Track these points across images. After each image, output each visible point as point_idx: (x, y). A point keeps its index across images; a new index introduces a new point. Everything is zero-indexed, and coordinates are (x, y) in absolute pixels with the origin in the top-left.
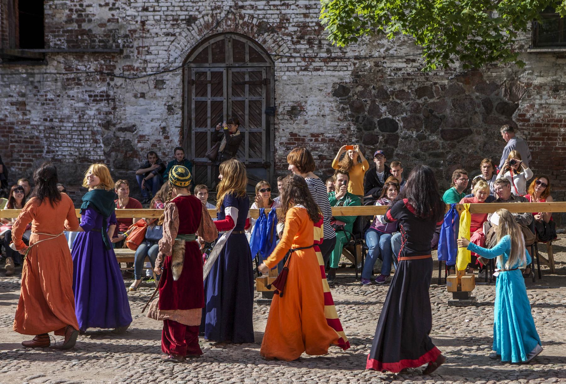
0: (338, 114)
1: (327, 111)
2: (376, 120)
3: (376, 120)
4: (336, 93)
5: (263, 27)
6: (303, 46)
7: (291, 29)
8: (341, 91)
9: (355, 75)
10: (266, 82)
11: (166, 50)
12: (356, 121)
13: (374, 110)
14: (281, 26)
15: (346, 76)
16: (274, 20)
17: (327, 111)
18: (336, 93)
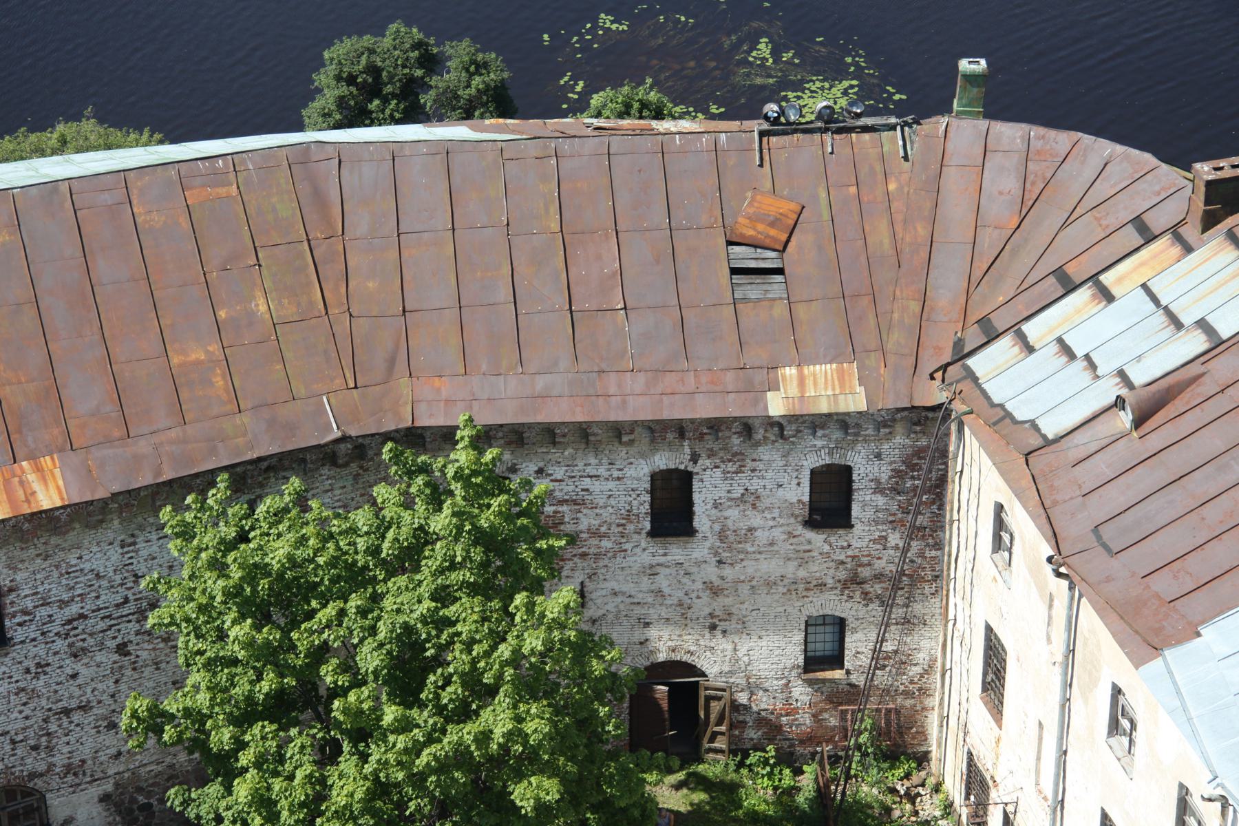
0: (105, 814)
1: (95, 814)
2: (135, 807)
3: (135, 807)
4: (101, 800)
5: (33, 775)
6: (70, 778)
7: (57, 770)
8: (105, 798)
9: (117, 785)
10: (38, 808)
12: (120, 813)
13: (133, 800)
14: (48, 771)
15: (109, 787)
16: (42, 767)
17: (95, 814)
18: (101, 800)
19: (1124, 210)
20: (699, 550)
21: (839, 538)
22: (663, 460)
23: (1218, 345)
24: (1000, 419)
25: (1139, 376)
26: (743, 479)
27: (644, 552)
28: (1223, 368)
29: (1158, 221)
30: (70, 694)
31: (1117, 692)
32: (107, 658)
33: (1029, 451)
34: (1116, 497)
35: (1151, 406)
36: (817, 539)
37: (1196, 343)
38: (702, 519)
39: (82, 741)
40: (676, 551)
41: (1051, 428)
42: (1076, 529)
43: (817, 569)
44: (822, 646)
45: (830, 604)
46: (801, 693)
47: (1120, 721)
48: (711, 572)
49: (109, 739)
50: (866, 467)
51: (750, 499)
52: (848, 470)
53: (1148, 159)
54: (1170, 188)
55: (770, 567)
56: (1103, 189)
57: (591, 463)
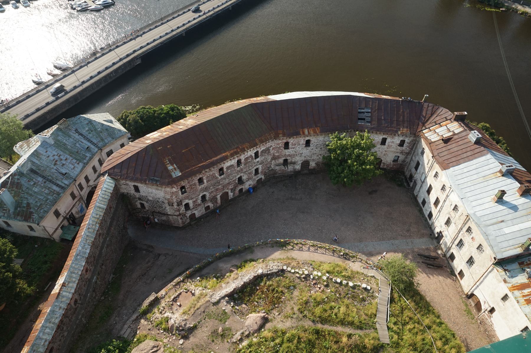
11: (300, 162)
19: (444, 116)
20: (385, 147)
21: (401, 148)
22: (384, 136)
23: (455, 134)
24: (426, 139)
25: (444, 136)
26: (393, 140)
27: (379, 146)
28: (456, 137)
29: (448, 118)
30: (315, 152)
31: (437, 172)
32: (319, 149)
33: (430, 143)
34: (440, 151)
35: (446, 141)
36: (399, 147)
37: (451, 134)
38: (386, 144)
39: (315, 157)
40: (383, 146)
41: (433, 140)
42: (436, 154)
43: (398, 151)
44: (396, 158)
45: (398, 155)
46: (392, 163)
47: (436, 175)
48: (386, 149)
49: (318, 158)
50: (407, 140)
51: (393, 142)
52: (405, 141)
53: (448, 110)
54: (449, 114)
55: (393, 150)
56: (442, 113)
57: (376, 136)
